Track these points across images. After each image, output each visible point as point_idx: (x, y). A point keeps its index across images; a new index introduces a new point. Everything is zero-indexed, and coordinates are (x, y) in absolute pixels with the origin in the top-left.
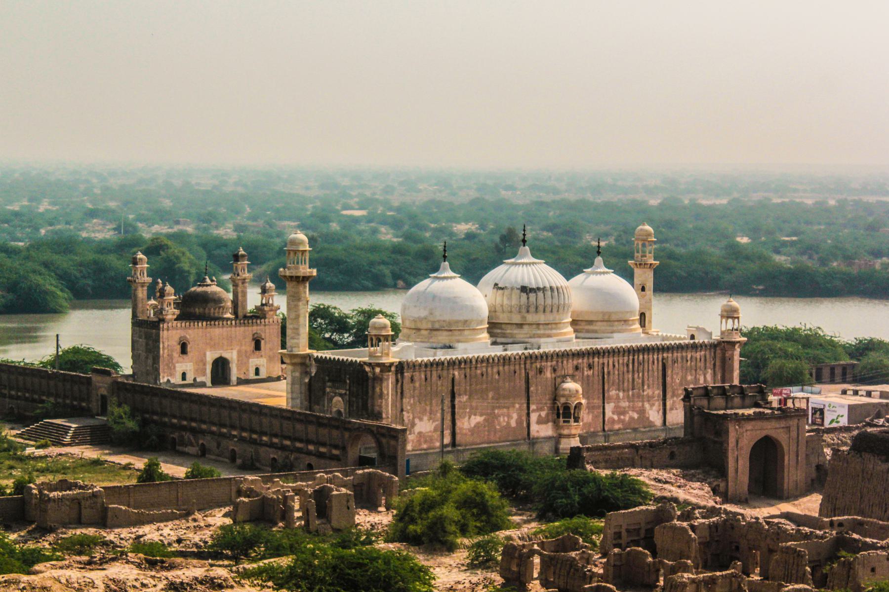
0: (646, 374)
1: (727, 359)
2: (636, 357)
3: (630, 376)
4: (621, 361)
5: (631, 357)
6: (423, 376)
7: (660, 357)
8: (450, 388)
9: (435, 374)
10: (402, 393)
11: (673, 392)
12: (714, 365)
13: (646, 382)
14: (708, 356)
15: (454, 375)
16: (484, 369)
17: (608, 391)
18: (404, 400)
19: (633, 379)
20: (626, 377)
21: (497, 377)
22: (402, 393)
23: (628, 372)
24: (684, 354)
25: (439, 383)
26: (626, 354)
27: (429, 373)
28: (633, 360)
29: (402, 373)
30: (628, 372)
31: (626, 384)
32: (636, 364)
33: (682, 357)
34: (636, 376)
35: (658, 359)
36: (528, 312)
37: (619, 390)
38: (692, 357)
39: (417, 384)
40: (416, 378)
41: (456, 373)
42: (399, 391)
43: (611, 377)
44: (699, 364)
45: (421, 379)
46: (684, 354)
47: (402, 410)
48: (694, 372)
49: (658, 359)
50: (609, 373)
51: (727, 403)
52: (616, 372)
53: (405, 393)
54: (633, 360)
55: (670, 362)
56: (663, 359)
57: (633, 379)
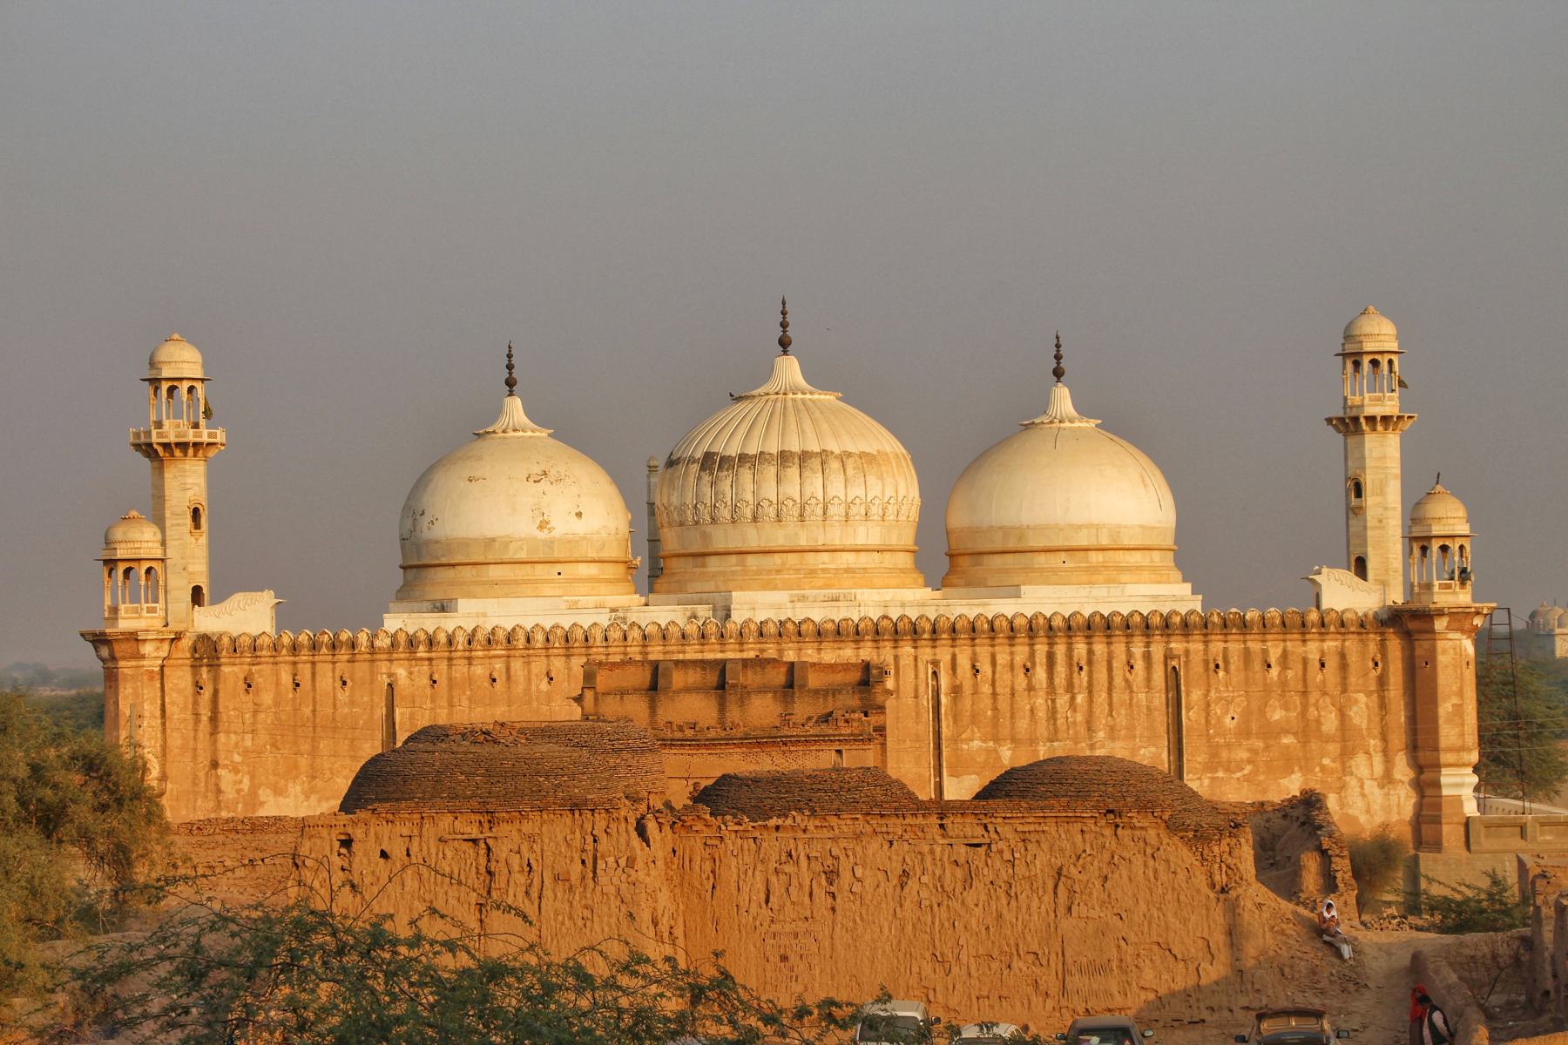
0: (1101, 697)
1: (1420, 663)
2: (1060, 650)
3: (1040, 701)
4: (1002, 659)
5: (1041, 649)
6: (286, 678)
7: (1157, 650)
8: (382, 711)
9: (325, 670)
10: (214, 719)
11: (1214, 752)
12: (1382, 682)
13: (1102, 721)
14: (1353, 659)
15: (390, 675)
16: (499, 666)
17: (955, 740)
18: (222, 737)
19: (1053, 713)
20: (1024, 704)
21: (544, 686)
22: (214, 719)
23: (1030, 688)
24: (1255, 646)
25: (343, 696)
26: (1022, 638)
27: (305, 670)
28: (1051, 658)
29: (214, 666)
30: (1030, 688)
31: (1023, 724)
32: (1061, 669)
33: (1247, 655)
34: (1062, 700)
35: (1147, 657)
36: (714, 520)
37: (997, 739)
38: (1285, 655)
39: (267, 698)
40: (258, 680)
41: (401, 672)
42: (205, 713)
43: (967, 702)
44: (1316, 677)
45: (278, 684)
46: (1255, 646)
47: (215, 765)
48: (1297, 700)
49: (1147, 657)
50: (956, 690)
51: (722, 708)
52: (986, 689)
53: (223, 717)
54: (1051, 658)
55: (1197, 667)
56: (1168, 656)
57: (1053, 713)
